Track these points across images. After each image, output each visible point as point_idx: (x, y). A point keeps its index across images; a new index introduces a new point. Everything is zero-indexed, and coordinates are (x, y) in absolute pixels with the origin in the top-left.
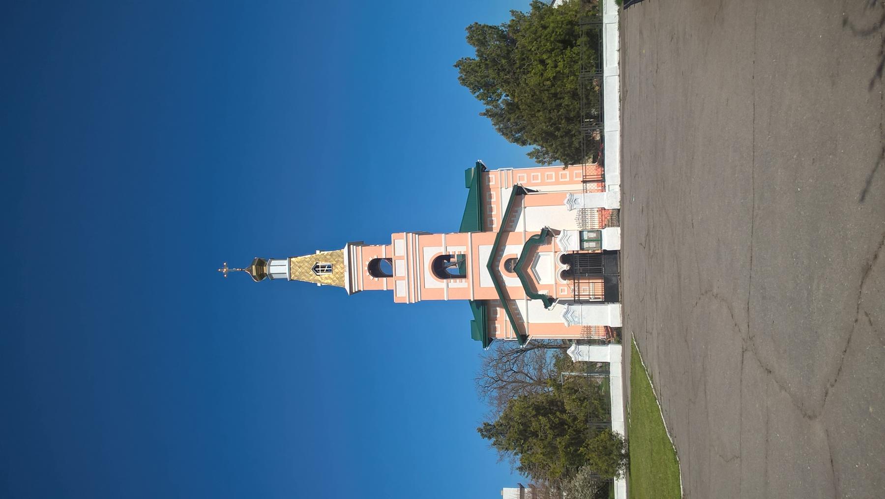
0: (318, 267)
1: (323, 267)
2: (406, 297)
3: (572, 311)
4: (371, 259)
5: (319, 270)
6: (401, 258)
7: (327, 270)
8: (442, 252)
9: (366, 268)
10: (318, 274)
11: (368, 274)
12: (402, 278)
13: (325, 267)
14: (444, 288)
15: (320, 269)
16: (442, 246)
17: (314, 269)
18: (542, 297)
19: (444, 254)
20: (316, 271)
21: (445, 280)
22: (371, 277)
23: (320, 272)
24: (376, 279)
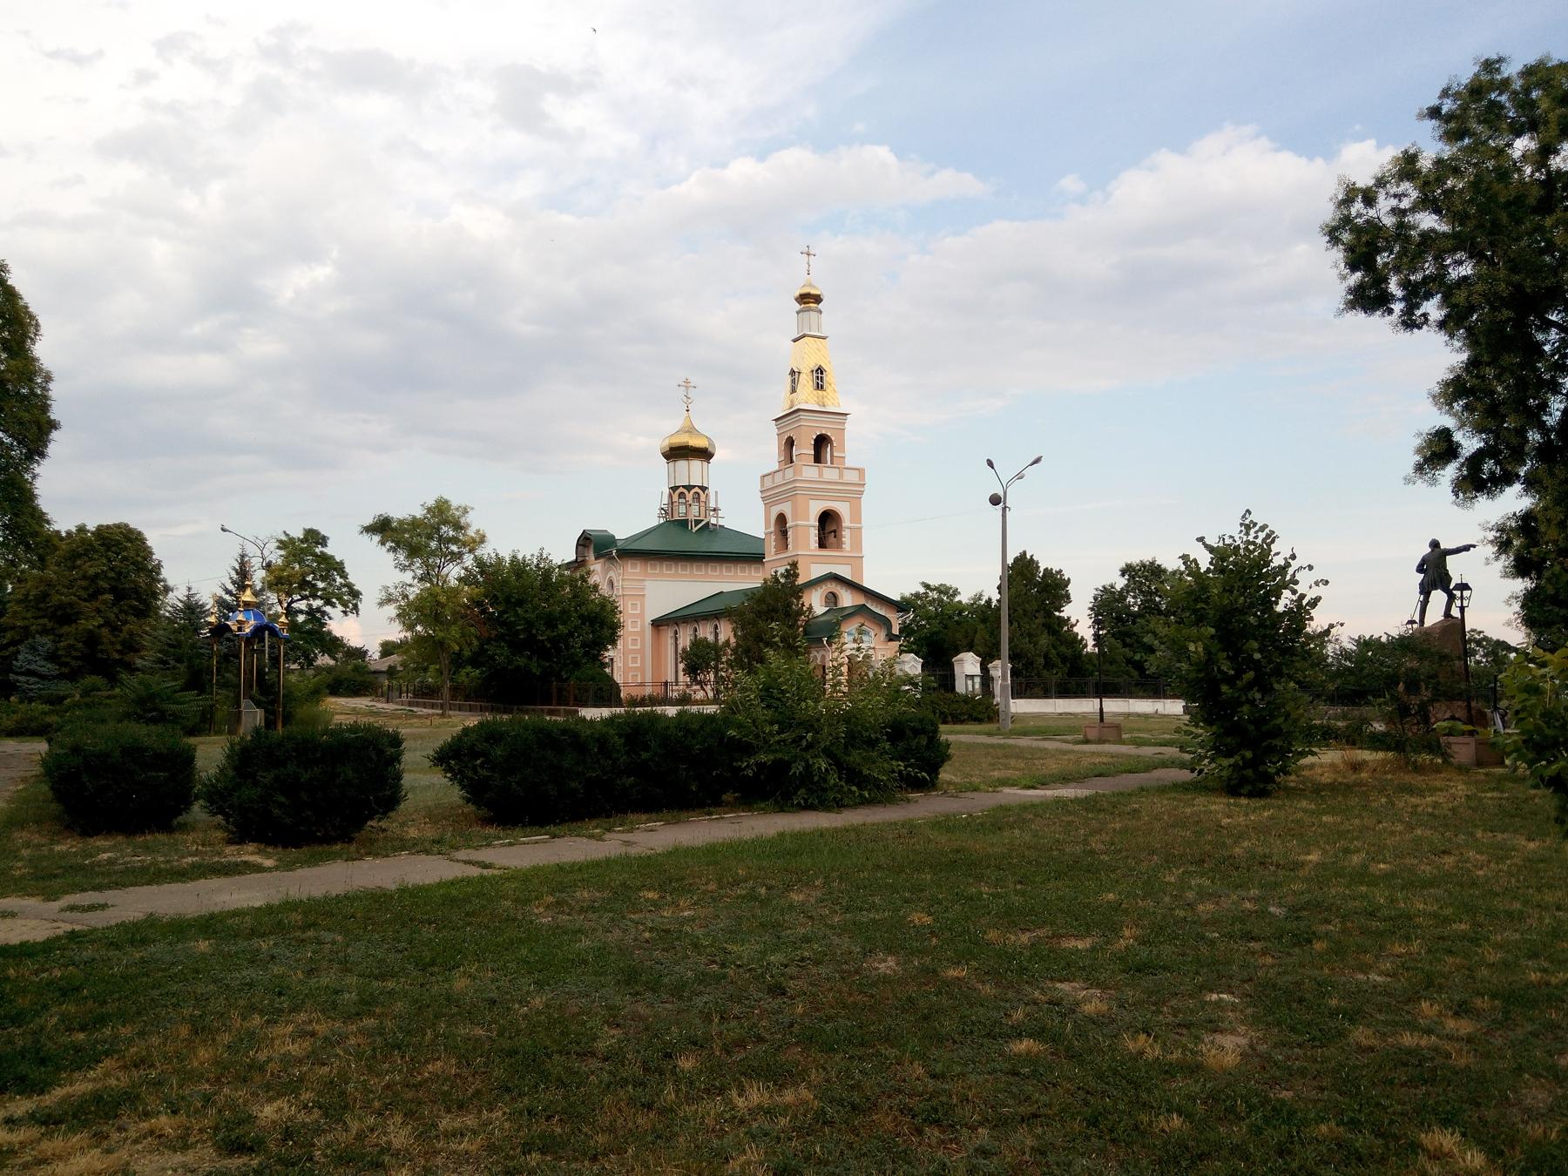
0: (822, 373)
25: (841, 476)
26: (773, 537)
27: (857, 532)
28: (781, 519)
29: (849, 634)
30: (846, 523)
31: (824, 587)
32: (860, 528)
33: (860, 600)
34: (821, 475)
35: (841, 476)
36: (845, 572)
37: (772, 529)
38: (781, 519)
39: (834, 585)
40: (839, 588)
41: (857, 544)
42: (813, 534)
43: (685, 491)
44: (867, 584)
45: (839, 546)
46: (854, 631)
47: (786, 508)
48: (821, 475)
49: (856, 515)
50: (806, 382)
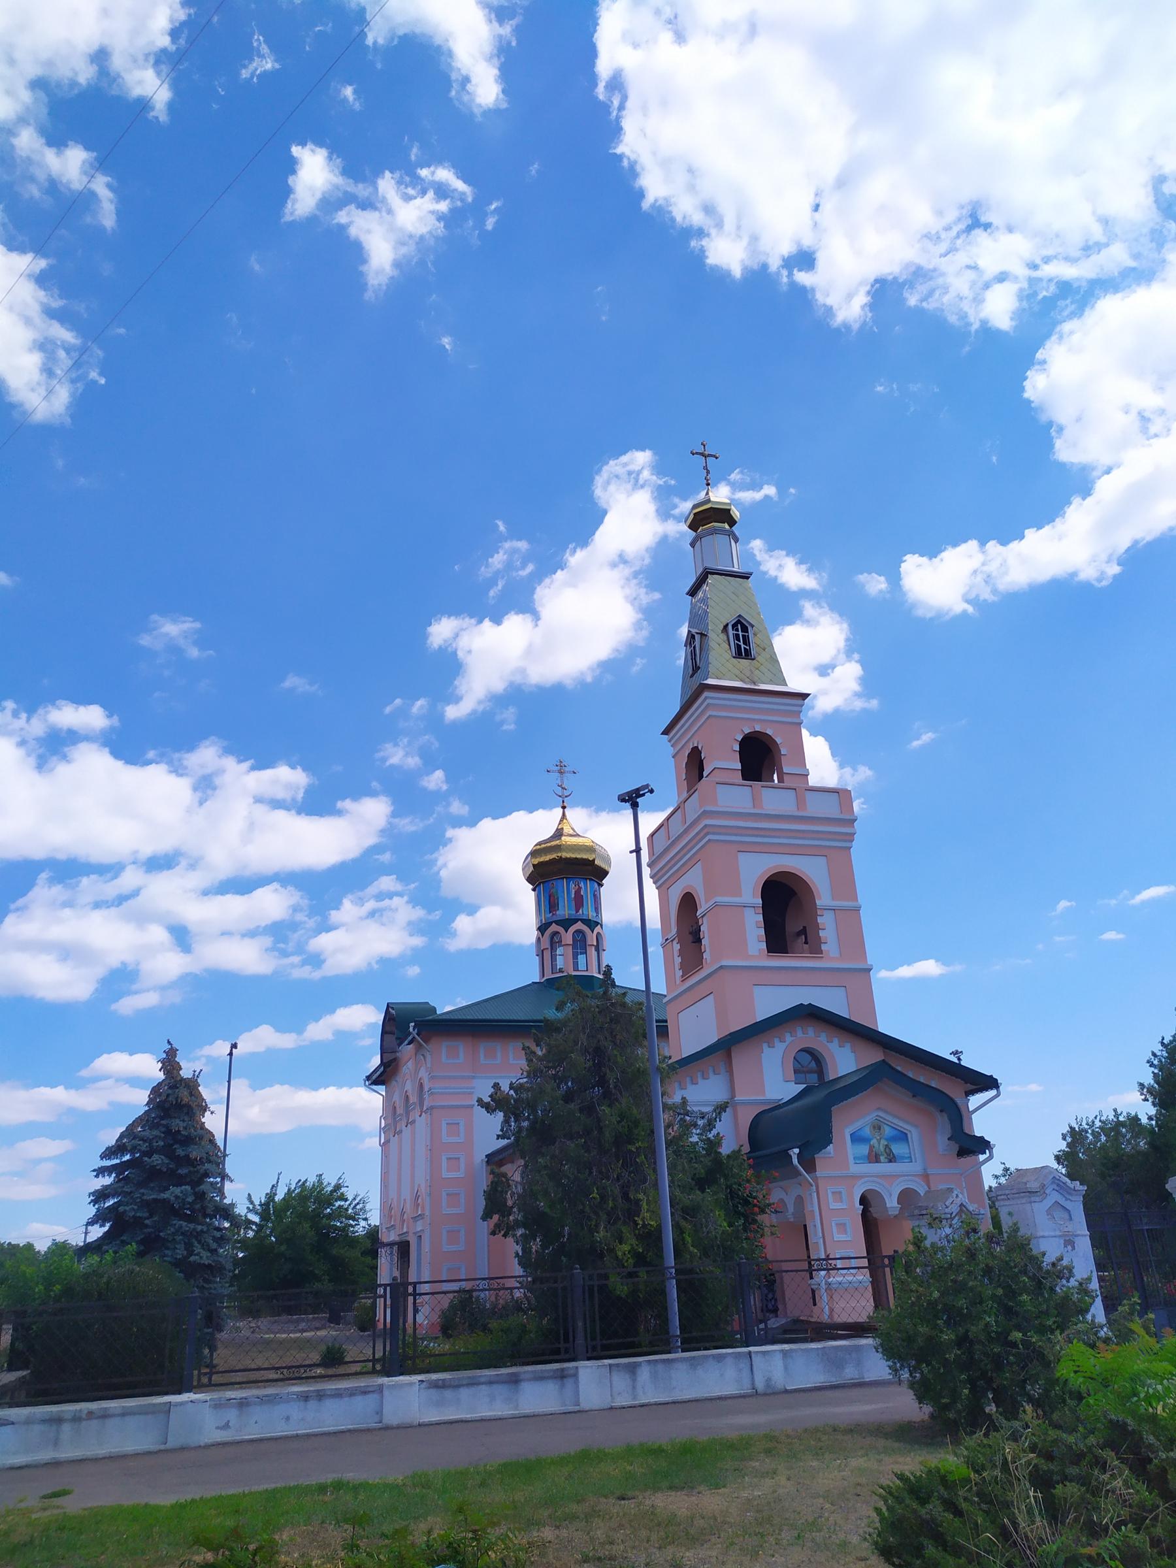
0: (745, 629)
1: (746, 640)
3: (1068, 1205)
4: (778, 740)
5: (737, 630)
7: (739, 647)
9: (758, 729)
10: (730, 627)
11: (747, 731)
13: (745, 643)
14: (741, 896)
16: (833, 899)
17: (739, 622)
24: (737, 748)
25: (801, 803)
26: (677, 947)
27: (851, 916)
28: (688, 902)
29: (856, 1138)
30: (824, 897)
31: (789, 1038)
32: (857, 910)
33: (873, 1056)
34: (756, 800)
35: (801, 803)
36: (833, 1001)
37: (674, 930)
38: (688, 902)
39: (811, 1031)
40: (823, 1037)
41: (854, 941)
42: (753, 926)
44: (883, 1028)
45: (815, 948)
47: (693, 880)
48: (756, 800)
49: (845, 882)
50: (719, 650)
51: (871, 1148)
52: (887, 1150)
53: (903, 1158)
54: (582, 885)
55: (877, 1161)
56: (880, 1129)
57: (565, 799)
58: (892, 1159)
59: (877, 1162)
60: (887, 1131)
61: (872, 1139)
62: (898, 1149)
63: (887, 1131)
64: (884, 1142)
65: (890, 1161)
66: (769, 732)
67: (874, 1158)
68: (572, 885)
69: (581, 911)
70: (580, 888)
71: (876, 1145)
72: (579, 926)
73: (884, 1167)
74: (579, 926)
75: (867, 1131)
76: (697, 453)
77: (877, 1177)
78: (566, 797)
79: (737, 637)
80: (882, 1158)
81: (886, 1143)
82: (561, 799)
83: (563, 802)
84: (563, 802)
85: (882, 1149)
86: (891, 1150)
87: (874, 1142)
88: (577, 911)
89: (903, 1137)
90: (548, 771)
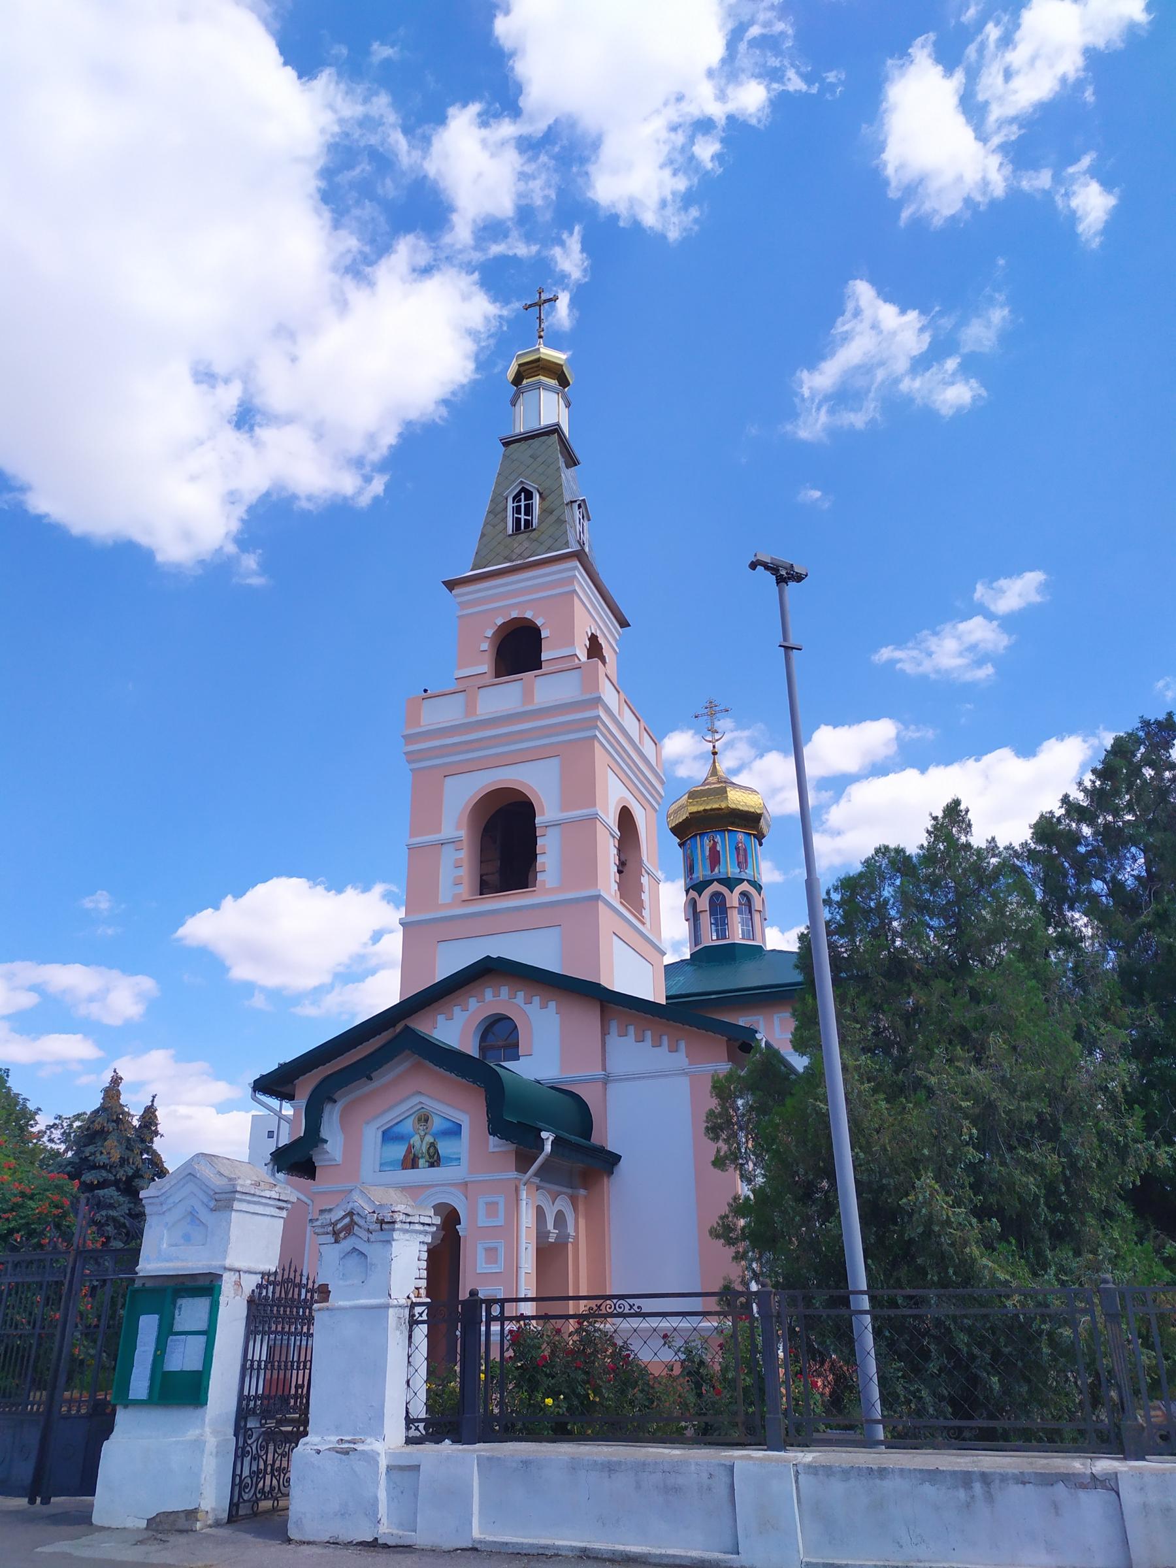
0: (529, 496)
1: (529, 510)
2: (421, 726)
4: (539, 622)
5: (520, 501)
6: (528, 695)
8: (543, 814)
9: (514, 614)
10: (510, 500)
11: (500, 621)
12: (470, 707)
15: (523, 504)
17: (523, 490)
18: (312, 1137)
19: (538, 820)
20: (519, 494)
21: (463, 833)
22: (489, 633)
23: (515, 504)
24: (485, 646)
31: (473, 1003)
43: (724, 890)
46: (408, 1126)
51: (410, 1147)
52: (432, 1150)
53: (451, 1159)
54: (718, 838)
55: (414, 1165)
56: (426, 1121)
57: (717, 744)
58: (435, 1160)
59: (413, 1168)
60: (437, 1124)
61: (413, 1136)
62: (444, 1148)
63: (437, 1124)
64: (429, 1139)
65: (432, 1165)
66: (528, 615)
67: (410, 1162)
68: (706, 841)
69: (716, 870)
70: (715, 843)
71: (417, 1144)
72: (715, 887)
73: (423, 1174)
74: (715, 887)
75: (408, 1126)
76: (531, 306)
77: (449, 1185)
78: (717, 740)
79: (518, 510)
80: (421, 1162)
81: (432, 1140)
82: (711, 745)
83: (714, 747)
84: (714, 747)
85: (424, 1150)
86: (437, 1151)
87: (416, 1140)
88: (712, 870)
89: (454, 1131)
90: (696, 717)
